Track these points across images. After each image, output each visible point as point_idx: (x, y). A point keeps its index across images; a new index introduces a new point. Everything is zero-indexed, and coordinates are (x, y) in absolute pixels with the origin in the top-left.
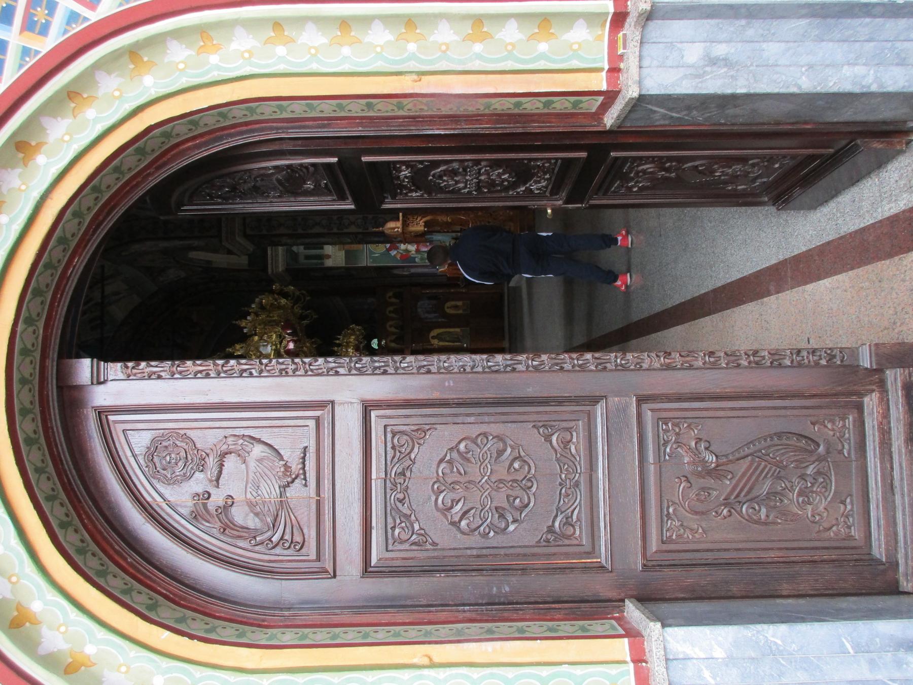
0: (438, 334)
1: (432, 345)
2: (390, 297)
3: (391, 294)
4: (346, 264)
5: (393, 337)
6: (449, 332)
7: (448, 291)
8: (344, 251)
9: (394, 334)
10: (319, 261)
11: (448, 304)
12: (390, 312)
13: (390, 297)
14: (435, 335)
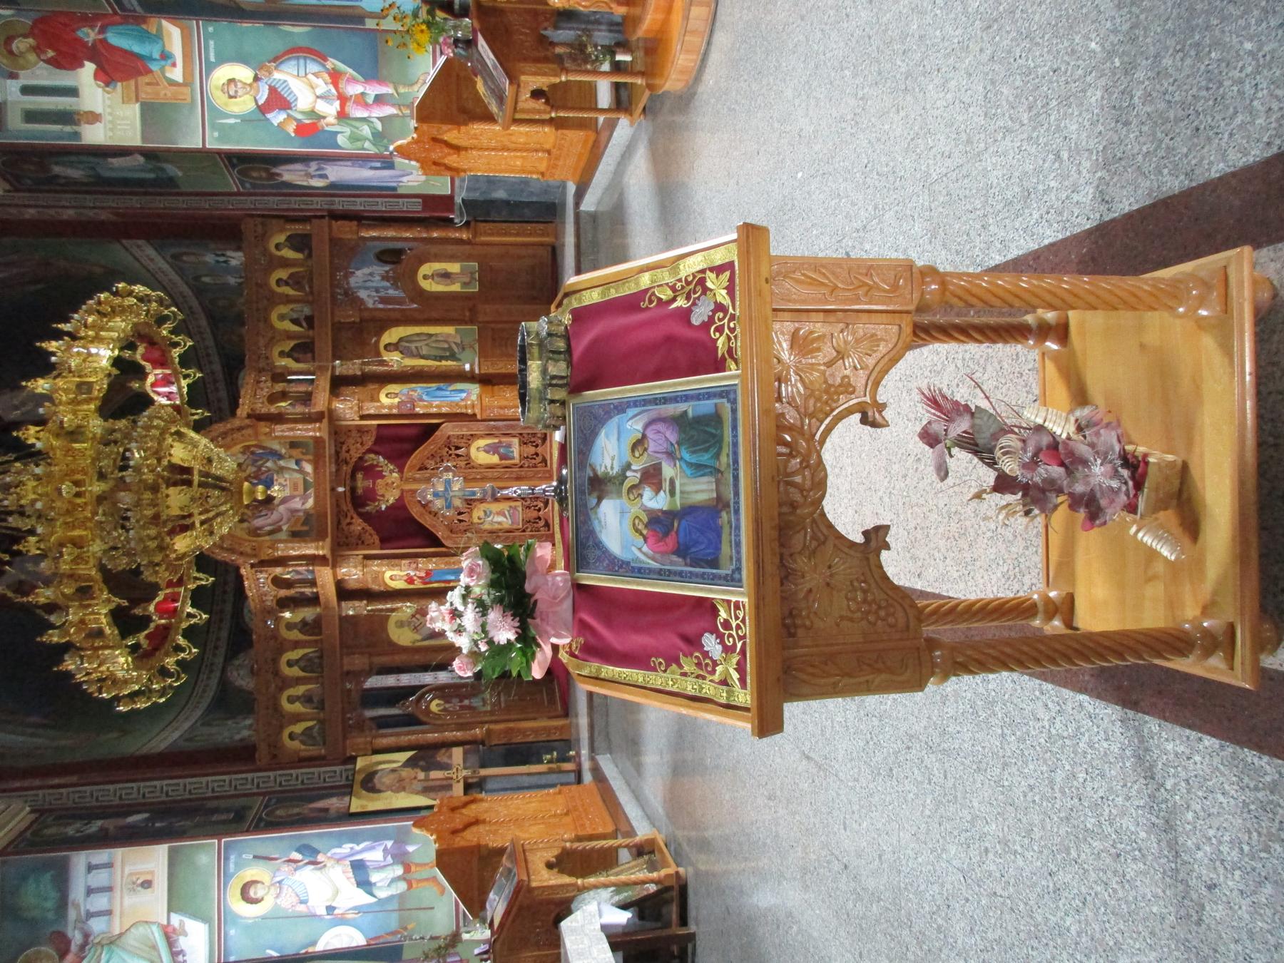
0: (401, 340)
1: (383, 363)
2: (278, 247)
3: (281, 238)
4: (144, 139)
6: (430, 336)
7: (425, 235)
8: (137, 106)
9: (289, 336)
10: (68, 129)
11: (426, 269)
12: (279, 282)
13: (278, 247)
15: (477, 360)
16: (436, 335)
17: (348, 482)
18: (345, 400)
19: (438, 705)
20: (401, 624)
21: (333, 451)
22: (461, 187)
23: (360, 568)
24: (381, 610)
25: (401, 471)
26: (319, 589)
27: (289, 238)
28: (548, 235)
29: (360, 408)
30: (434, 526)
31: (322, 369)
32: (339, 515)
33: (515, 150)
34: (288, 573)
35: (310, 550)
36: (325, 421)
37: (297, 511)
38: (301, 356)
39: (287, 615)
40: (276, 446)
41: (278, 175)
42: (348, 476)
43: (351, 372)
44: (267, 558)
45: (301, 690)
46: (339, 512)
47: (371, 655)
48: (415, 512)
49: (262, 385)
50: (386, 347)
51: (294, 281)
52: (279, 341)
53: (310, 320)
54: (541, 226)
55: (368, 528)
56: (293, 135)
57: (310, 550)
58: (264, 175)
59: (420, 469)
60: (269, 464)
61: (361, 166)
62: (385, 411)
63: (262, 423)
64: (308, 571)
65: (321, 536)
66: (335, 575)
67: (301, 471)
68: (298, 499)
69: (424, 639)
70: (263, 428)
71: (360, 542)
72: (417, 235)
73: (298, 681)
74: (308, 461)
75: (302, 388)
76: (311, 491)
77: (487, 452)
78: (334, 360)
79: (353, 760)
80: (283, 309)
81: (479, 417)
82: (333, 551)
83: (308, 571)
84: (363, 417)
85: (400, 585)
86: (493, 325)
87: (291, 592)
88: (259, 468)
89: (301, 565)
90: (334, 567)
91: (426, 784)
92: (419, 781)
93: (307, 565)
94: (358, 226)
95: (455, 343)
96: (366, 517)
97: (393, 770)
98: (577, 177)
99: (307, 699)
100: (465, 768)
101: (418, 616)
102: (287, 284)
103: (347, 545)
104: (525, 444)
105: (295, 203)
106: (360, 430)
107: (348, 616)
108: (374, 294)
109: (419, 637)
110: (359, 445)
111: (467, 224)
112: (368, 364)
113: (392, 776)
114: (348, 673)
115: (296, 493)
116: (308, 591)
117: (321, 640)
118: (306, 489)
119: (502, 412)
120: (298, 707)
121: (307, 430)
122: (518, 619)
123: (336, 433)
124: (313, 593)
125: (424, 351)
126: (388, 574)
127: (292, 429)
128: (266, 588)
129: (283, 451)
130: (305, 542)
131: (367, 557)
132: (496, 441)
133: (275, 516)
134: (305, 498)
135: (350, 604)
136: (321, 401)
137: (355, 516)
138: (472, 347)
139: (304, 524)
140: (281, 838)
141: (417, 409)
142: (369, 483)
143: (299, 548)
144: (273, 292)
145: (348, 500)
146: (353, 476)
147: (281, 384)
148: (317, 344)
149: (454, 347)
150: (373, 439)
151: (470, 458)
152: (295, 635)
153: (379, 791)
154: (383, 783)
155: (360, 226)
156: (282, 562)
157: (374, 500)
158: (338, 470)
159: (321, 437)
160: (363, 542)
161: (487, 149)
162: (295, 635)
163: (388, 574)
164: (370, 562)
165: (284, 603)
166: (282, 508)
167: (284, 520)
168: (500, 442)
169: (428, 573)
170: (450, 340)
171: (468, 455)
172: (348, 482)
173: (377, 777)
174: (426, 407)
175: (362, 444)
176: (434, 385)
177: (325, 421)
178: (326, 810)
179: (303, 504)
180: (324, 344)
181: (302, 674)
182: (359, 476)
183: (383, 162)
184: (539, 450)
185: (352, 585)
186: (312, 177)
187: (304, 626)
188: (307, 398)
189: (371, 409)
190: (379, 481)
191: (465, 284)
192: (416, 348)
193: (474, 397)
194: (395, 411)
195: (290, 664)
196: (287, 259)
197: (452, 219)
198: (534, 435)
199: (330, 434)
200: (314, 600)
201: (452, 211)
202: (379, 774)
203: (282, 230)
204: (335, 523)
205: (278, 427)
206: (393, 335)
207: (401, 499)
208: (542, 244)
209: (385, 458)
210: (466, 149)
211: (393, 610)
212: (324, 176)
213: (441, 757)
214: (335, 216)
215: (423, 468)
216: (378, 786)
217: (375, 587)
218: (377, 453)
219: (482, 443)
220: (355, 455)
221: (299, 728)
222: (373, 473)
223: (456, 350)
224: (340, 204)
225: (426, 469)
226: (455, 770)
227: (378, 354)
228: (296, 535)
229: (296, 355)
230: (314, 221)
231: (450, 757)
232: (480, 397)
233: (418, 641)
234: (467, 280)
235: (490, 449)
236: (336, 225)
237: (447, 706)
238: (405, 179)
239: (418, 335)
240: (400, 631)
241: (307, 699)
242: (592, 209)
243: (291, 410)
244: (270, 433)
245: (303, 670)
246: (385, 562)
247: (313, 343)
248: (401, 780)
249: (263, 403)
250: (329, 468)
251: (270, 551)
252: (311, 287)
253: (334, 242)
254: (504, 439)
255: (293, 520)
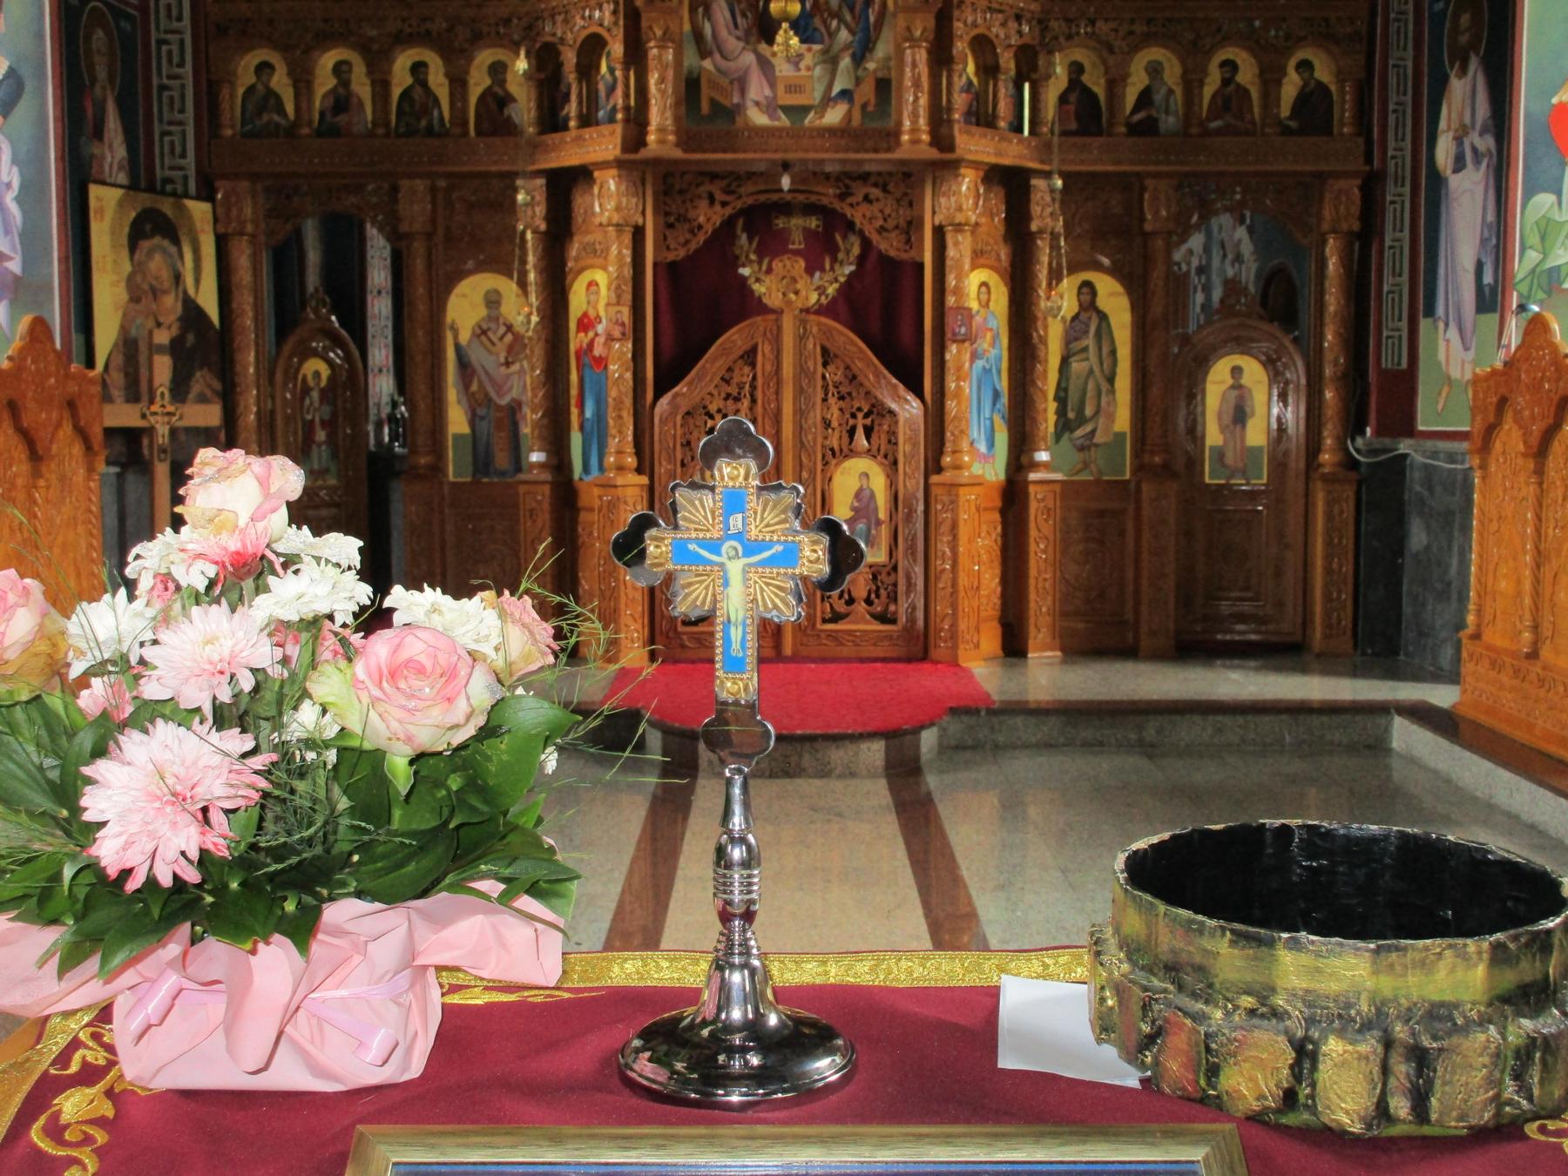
0: (1103, 317)
1: (1055, 276)
2: (1305, 66)
5: (1095, 82)
6: (1111, 380)
7: (1328, 371)
9: (1115, 83)
11: (1254, 372)
12: (1230, 66)
13: (1305, 66)
14: (1103, 302)
15: (1058, 476)
16: (1112, 391)
17: (801, 197)
18: (978, 196)
19: (317, 374)
20: (493, 300)
21: (867, 168)
22: (1434, 455)
23: (616, 218)
24: (524, 262)
25: (820, 310)
26: (573, 133)
27: (1322, 87)
28: (1326, 637)
29: (959, 228)
30: (700, 378)
31: (1045, 150)
32: (733, 179)
33: (1537, 581)
34: (611, 70)
35: (659, 115)
36: (934, 154)
37: (743, 92)
38: (1072, 108)
39: (522, 65)
40: (882, 49)
41: (1463, 71)
42: (813, 198)
43: (1036, 210)
44: (644, 24)
45: (362, 88)
46: (738, 177)
47: (429, 236)
48: (734, 338)
49: (1013, 25)
50: (1088, 285)
51: (1231, 98)
52: (1104, 62)
53: (1145, 128)
54: (1347, 622)
55: (701, 238)
56: (1555, 100)
57: (659, 115)
58: (1464, 39)
59: (825, 351)
60: (844, 35)
61: (1484, 242)
62: (951, 281)
63: (931, 23)
64: (614, 110)
65: (687, 139)
66: (604, 165)
67: (827, 101)
68: (768, 92)
69: (458, 347)
70: (923, 25)
71: (670, 221)
72: (1329, 356)
73: (381, 86)
74: (849, 112)
75: (1004, 108)
76: (784, 121)
77: (858, 495)
78: (1063, 175)
79: (207, 194)
80: (1172, 72)
81: (934, 479)
82: (656, 162)
83: (614, 110)
84: (939, 232)
85: (578, 301)
86: (1131, 508)
87: (571, 77)
88: (837, 15)
89: (626, 96)
90: (619, 164)
91: (143, 347)
92: (151, 333)
93: (627, 108)
94: (1350, 233)
95: (1093, 432)
96: (725, 232)
97: (178, 278)
98: (1470, 714)
99: (342, 101)
100: (173, 432)
101: (509, 337)
102: (1226, 82)
103: (666, 193)
104: (875, 577)
105: (1399, 99)
106: (912, 228)
107: (516, 190)
108: (1195, 262)
109: (464, 337)
110: (880, 222)
111: (1351, 464)
112: (1054, 247)
113: (166, 275)
114: (395, 189)
115: (781, 89)
116: (572, 108)
117: (465, 134)
118: (788, 110)
119: (945, 528)
120: (324, 82)
121: (915, 116)
122: (192, 875)
123: (907, 175)
124: (567, 119)
125: (1076, 366)
126: (601, 277)
127: (917, 84)
128: (580, 23)
129: (871, 66)
130: (677, 104)
131: (638, 233)
132: (882, 515)
133: (732, 43)
134: (770, 107)
135: (541, 197)
136: (976, 146)
137: (728, 211)
138: (1086, 465)
139: (713, 102)
140: (40, 36)
141: (954, 348)
142: (797, 243)
143: (663, 92)
144: (1208, 54)
145: (762, 198)
146: (810, 209)
147: (1012, 65)
148: (1097, 141)
149: (1088, 428)
150: (892, 253)
151: (846, 457)
152: (479, 81)
153: (133, 247)
154: (150, 255)
155: (1350, 237)
156: (635, 56)
157: (761, 255)
158: (827, 177)
159: (898, 143)
160: (670, 226)
161: (1538, 517)
162: (479, 81)
163: (601, 277)
164: (627, 238)
165: (546, 61)
166: (749, 58)
167: (723, 64)
168: (879, 523)
169: (601, 362)
170: (1102, 420)
171: (851, 453)
172: (801, 197)
173: (166, 243)
174: (959, 368)
175: (881, 230)
176: (1003, 385)
177: (934, 154)
178: (99, 133)
179: (757, 104)
180: (1096, 158)
181: (396, 92)
182: (813, 223)
183: (1493, 289)
184: (861, 607)
185: (579, 201)
186: (1459, 140)
187: (497, 99)
188: (981, 117)
189: (959, 248)
190: (802, 263)
191: (1219, 454)
192: (1085, 349)
193: (977, 469)
194: (951, 301)
195: (418, 69)
196: (1279, 83)
197: (1363, 433)
198: (893, 598)
199: (903, 162)
200: (552, 121)
201: (1378, 433)
202: (173, 249)
203: (1341, 77)
204: (715, 169)
205: (922, 56)
206: (1113, 298)
207: (761, 308)
208: (1306, 622)
209: (851, 276)
210: (1540, 471)
211: (523, 284)
212: (1459, 164)
213: (202, 381)
214: (1372, 186)
215: (827, 357)
216: (145, 245)
217: (574, 250)
218: (861, 260)
219: (879, 483)
220: (858, 215)
221: (280, 81)
222: (820, 251)
223: (1079, 433)
224: (1396, 197)
225: (825, 364)
226: (171, 409)
227: (1074, 269)
228: (691, 87)
229: (1073, 98)
230: (1361, 140)
231: (202, 399)
232: (977, 483)
233: (456, 337)
234: (1229, 459)
235: (863, 501)
236: (1353, 188)
237: (315, 395)
238: (1453, 333)
239: (1113, 352)
240: (479, 299)
241: (342, 101)
242: (1395, 744)
243: (959, 83)
244: (911, 39)
245: (406, 94)
246: (628, 272)
247: (1099, 133)
248: (155, 293)
249: (975, 25)
250: (832, 159)
251: (659, 33)
252: (1219, 132)
253: (1312, 186)
254: (884, 532)
255: (724, 82)
